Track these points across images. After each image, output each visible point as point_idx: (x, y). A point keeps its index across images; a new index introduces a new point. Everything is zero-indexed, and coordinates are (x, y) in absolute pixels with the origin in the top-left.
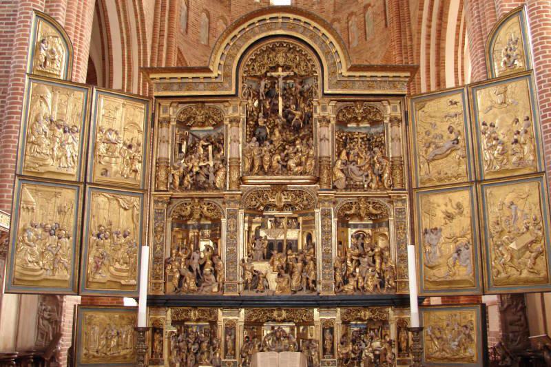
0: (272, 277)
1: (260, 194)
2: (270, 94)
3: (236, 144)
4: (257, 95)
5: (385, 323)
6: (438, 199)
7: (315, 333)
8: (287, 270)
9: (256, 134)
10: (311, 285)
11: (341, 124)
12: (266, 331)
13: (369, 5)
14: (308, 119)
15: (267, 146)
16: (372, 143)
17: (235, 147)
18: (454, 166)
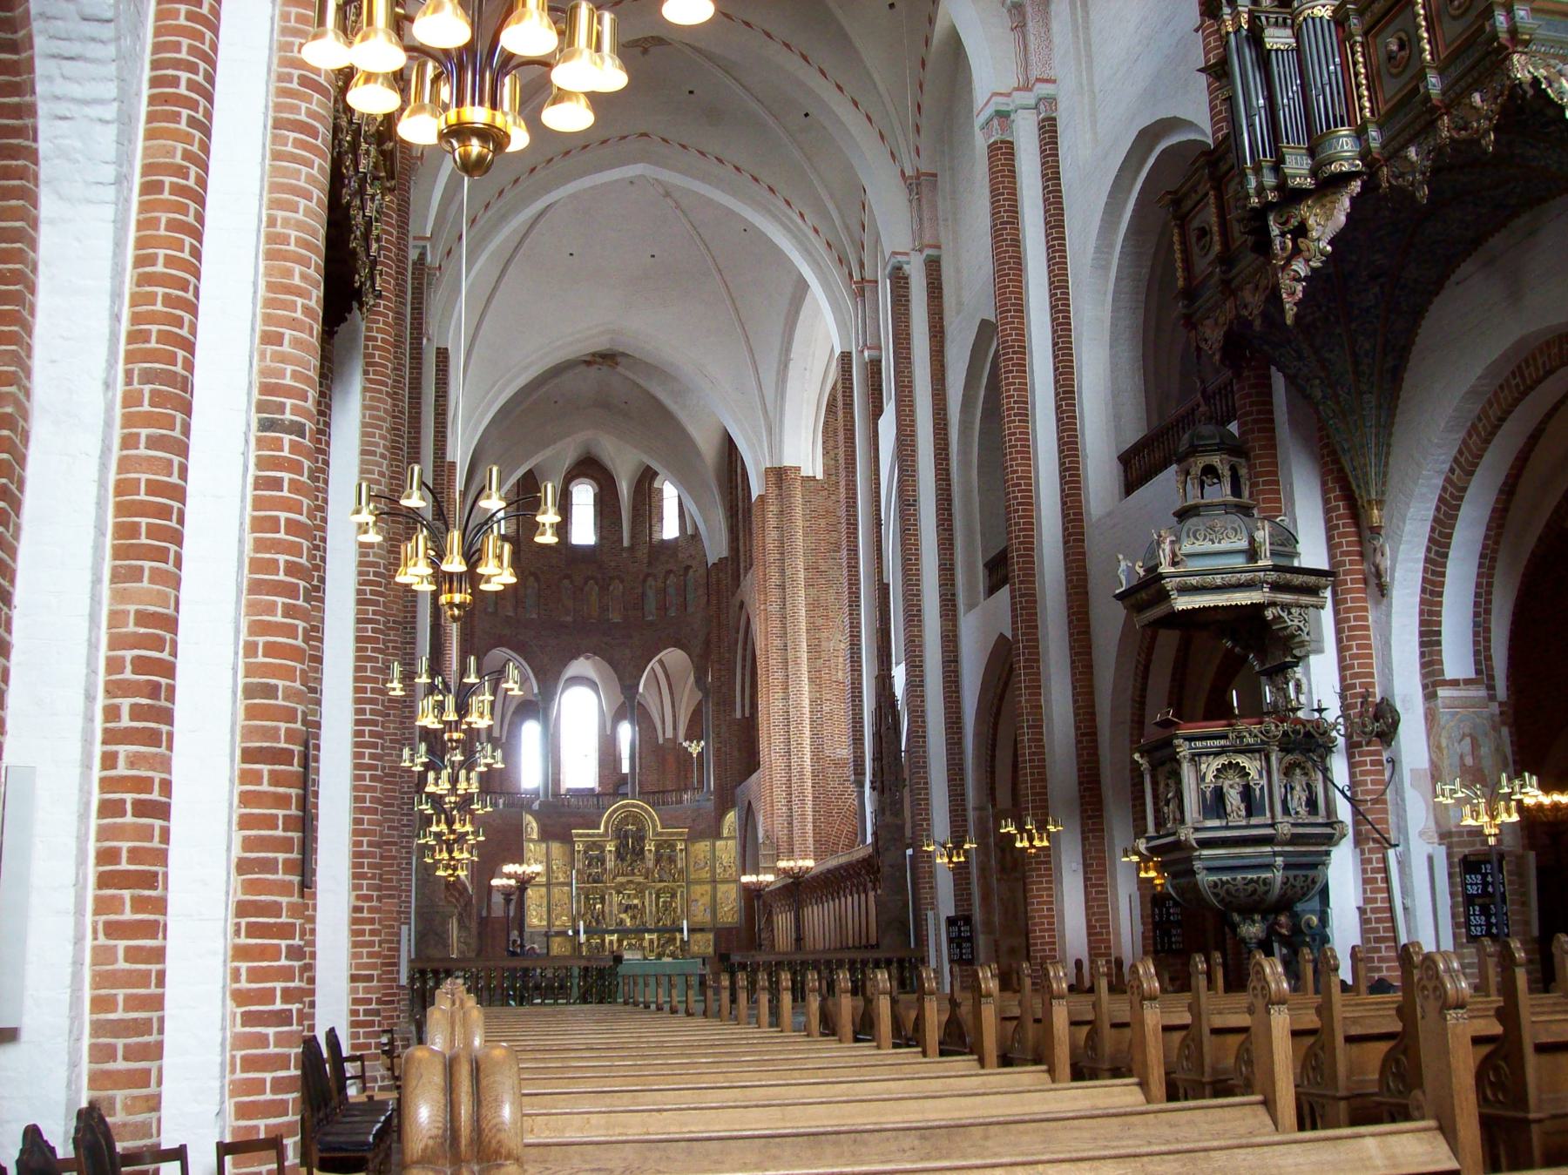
0: (628, 920)
1: (622, 884)
2: (626, 837)
3: (610, 863)
4: (618, 837)
5: (675, 939)
6: (698, 887)
7: (646, 944)
8: (633, 918)
9: (619, 855)
10: (644, 924)
11: (657, 851)
12: (625, 943)
13: (690, 567)
14: (642, 849)
15: (625, 864)
16: (672, 860)
17: (610, 863)
18: (705, 875)
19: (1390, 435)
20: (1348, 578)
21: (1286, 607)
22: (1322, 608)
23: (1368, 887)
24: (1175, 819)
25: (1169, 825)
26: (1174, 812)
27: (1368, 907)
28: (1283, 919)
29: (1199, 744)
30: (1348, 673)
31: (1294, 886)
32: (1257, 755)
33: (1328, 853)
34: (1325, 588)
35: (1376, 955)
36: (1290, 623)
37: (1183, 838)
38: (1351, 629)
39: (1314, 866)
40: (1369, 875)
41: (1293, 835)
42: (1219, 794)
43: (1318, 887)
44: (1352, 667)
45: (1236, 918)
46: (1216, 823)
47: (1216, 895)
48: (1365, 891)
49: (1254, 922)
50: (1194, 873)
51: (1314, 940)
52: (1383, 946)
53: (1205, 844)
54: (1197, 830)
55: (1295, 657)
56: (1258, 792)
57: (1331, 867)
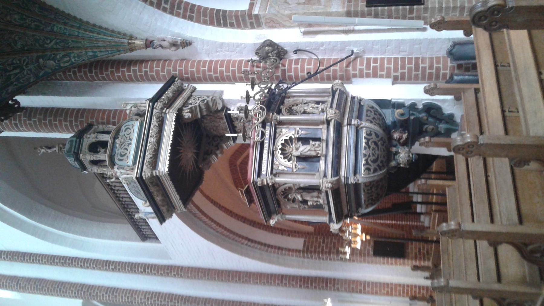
19: (87, 23)
20: (178, 68)
21: (185, 104)
22: (195, 89)
23: (379, 73)
24: (318, 197)
25: (321, 202)
26: (312, 197)
27: (393, 74)
28: (396, 136)
29: (264, 168)
30: (237, 75)
31: (374, 118)
32: (278, 130)
33: (353, 98)
34: (182, 84)
35: (428, 71)
36: (197, 104)
37: (330, 185)
38: (210, 70)
39: (361, 107)
40: (371, 71)
41: (338, 107)
42: (302, 158)
43: (376, 106)
44: (233, 72)
45: (393, 163)
46: (322, 163)
47: (375, 171)
48: (382, 76)
49: (397, 153)
50: (357, 185)
51: (413, 114)
52: (421, 65)
53: (336, 171)
54: (325, 176)
55: (222, 109)
56: (303, 132)
57: (362, 97)
